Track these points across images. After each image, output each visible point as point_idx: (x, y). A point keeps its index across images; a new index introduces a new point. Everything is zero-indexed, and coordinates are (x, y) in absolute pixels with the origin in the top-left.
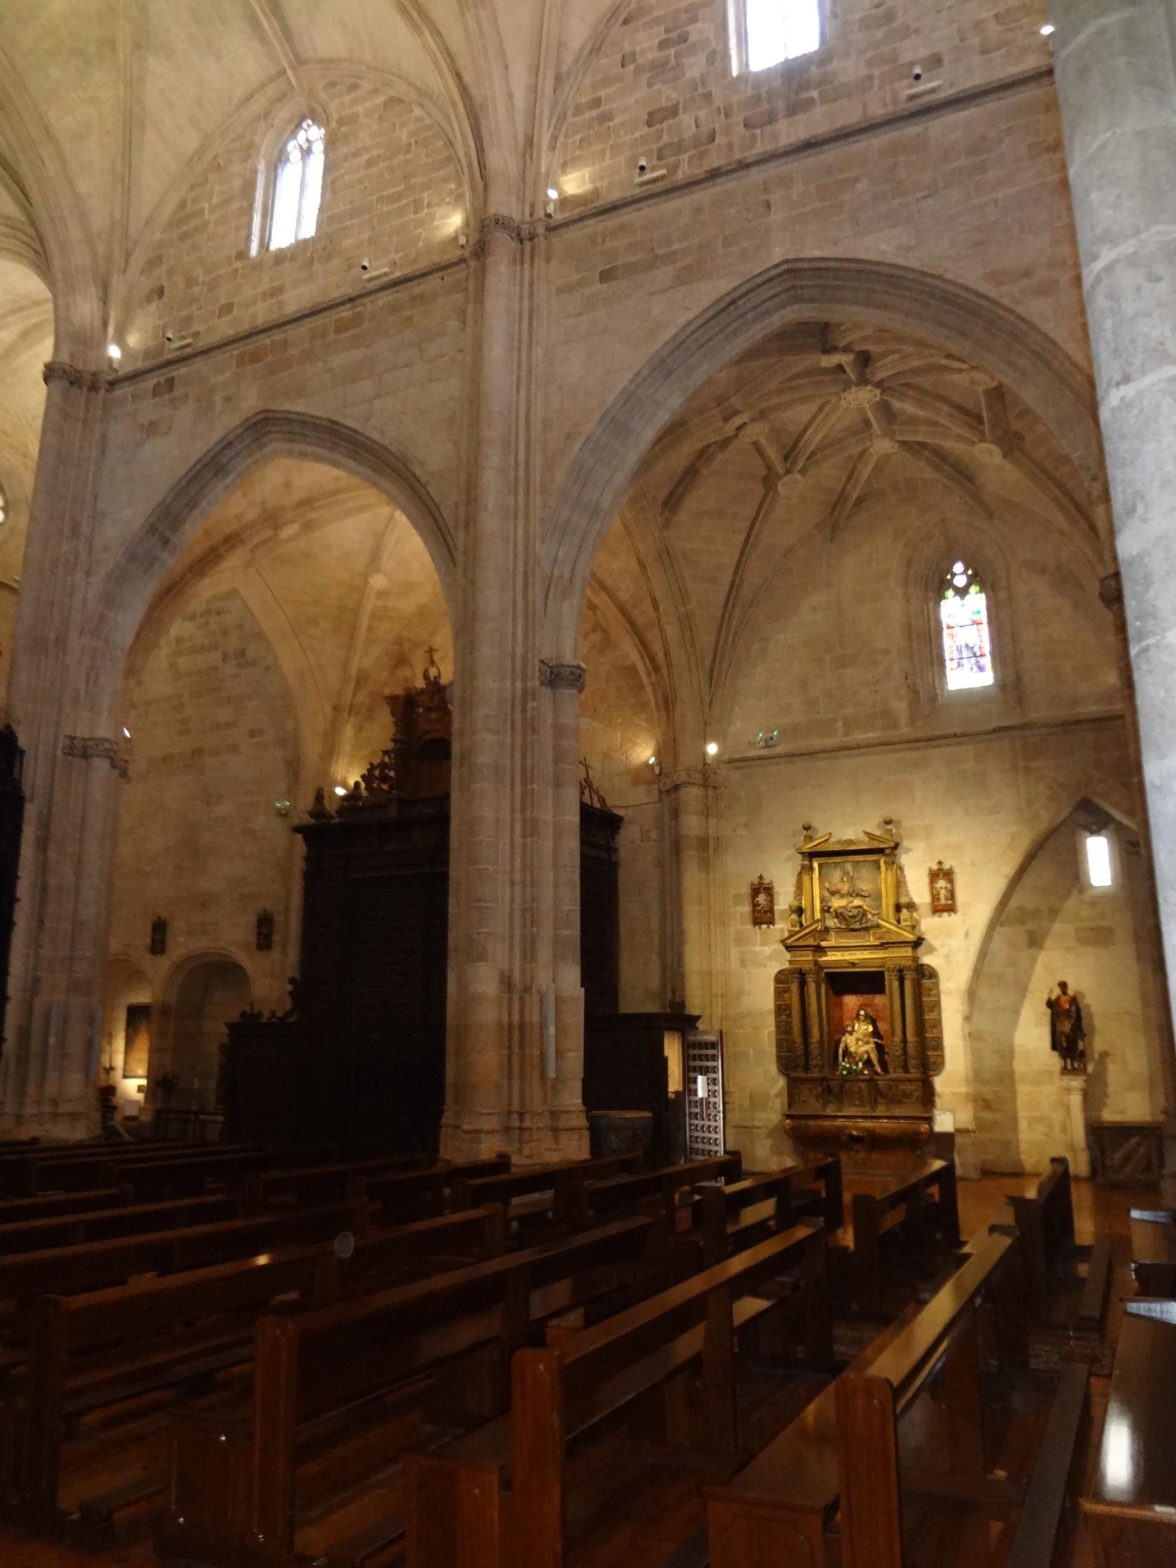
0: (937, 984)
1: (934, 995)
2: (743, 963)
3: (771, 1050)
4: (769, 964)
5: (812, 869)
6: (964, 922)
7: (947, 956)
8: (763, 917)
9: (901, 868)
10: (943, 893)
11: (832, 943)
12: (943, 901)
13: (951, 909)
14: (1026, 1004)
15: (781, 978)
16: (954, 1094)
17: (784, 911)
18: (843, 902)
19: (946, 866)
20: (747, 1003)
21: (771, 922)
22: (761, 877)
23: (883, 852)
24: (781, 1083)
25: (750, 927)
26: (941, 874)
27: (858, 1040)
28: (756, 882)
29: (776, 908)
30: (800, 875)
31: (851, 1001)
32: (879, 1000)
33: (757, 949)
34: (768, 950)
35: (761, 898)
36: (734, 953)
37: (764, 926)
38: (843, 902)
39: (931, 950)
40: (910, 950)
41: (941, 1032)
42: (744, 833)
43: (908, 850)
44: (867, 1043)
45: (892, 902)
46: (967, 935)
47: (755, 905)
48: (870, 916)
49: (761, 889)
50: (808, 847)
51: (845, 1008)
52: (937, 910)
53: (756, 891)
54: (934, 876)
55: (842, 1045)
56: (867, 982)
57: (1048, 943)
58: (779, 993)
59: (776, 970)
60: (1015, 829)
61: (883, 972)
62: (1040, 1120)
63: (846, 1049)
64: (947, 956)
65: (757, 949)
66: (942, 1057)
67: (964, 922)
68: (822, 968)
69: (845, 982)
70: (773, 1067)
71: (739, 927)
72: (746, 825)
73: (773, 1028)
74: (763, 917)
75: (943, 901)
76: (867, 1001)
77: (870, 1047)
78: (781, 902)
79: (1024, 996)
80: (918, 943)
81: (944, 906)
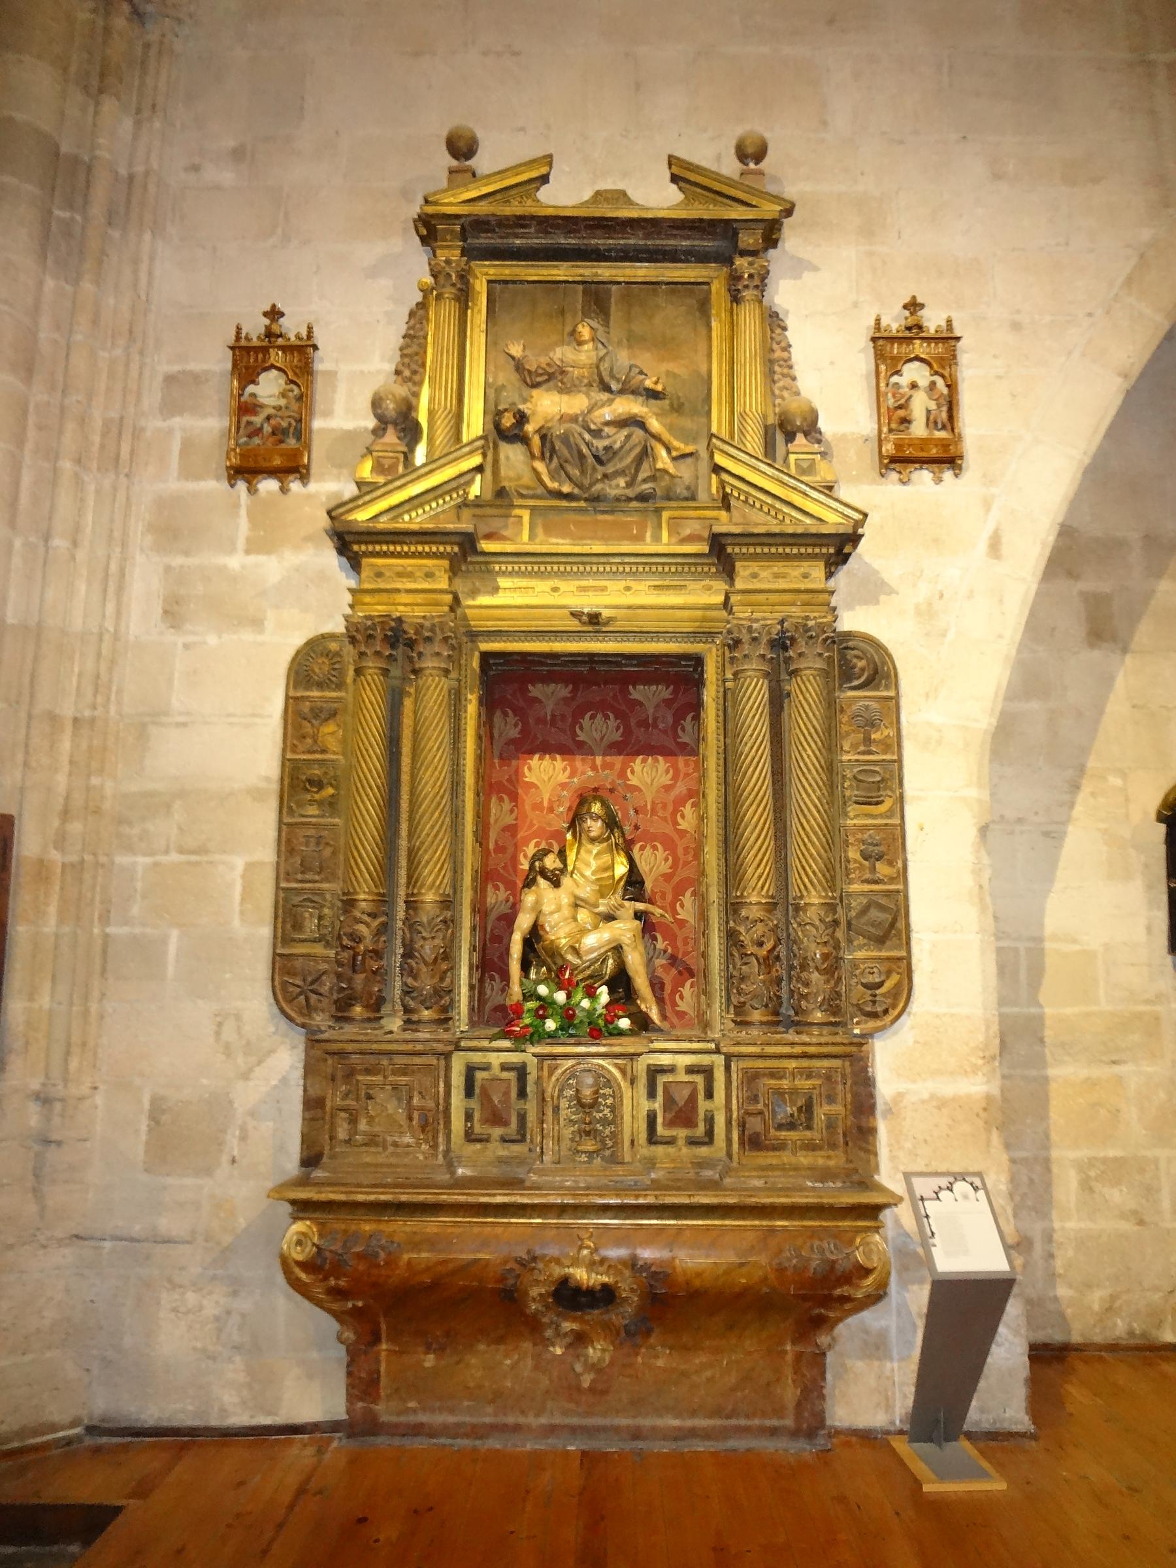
0: (893, 705)
1: (886, 746)
2: (173, 613)
3: (255, 934)
4: (271, 617)
5: (464, 297)
6: (987, 505)
7: (926, 613)
8: (268, 452)
9: (773, 321)
10: (920, 405)
11: (523, 541)
12: (919, 429)
13: (947, 459)
14: (1078, 810)
15: (312, 668)
16: (941, 1103)
17: (349, 437)
18: (577, 403)
19: (933, 320)
20: (173, 757)
21: (294, 469)
22: (274, 314)
23: (722, 241)
24: (285, 1061)
25: (214, 486)
26: (910, 343)
27: (577, 909)
28: (255, 327)
29: (317, 424)
30: (419, 313)
31: (547, 775)
32: (647, 775)
33: (235, 562)
34: (273, 568)
35: (269, 388)
36: (146, 577)
37: (268, 486)
38: (577, 403)
39: (874, 590)
40: (817, 571)
41: (902, 875)
42: (227, 177)
43: (800, 267)
44: (610, 918)
45: (753, 401)
46: (995, 546)
47: (245, 408)
48: (663, 459)
49: (273, 351)
50: (455, 202)
51: (527, 802)
52: (900, 460)
53: (248, 359)
54: (890, 348)
55: (524, 922)
56: (618, 697)
57: (1144, 633)
58: (300, 720)
59: (298, 640)
60: (1146, 234)
61: (698, 661)
62: (1116, 1170)
63: (534, 936)
64: (926, 613)
65: (235, 562)
66: (904, 966)
67: (987, 505)
68: (474, 636)
69: (548, 695)
70: (255, 1000)
71: (174, 485)
72: (238, 154)
73: (267, 854)
74: (268, 452)
75: (919, 429)
76: (608, 778)
77: (625, 929)
78: (339, 406)
79: (1075, 787)
80: (839, 547)
81: (924, 449)
